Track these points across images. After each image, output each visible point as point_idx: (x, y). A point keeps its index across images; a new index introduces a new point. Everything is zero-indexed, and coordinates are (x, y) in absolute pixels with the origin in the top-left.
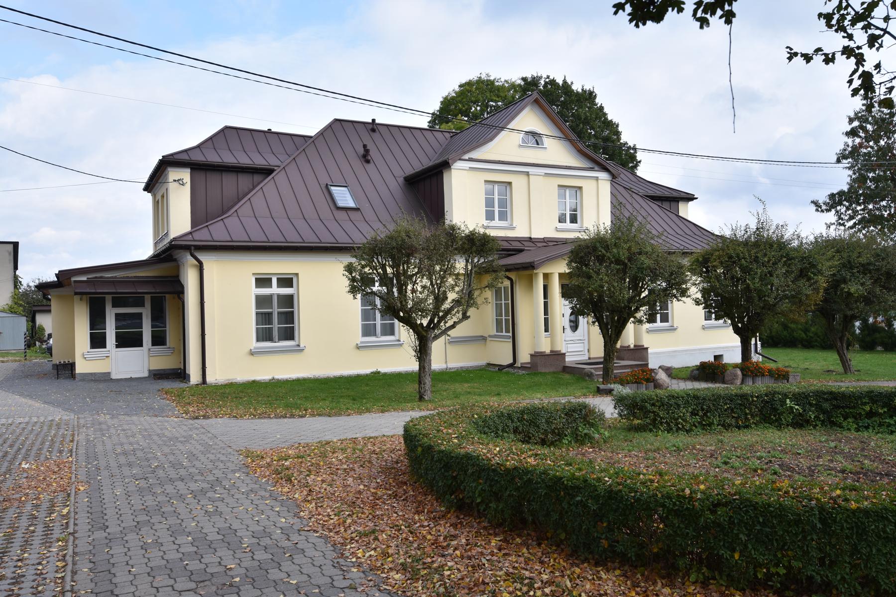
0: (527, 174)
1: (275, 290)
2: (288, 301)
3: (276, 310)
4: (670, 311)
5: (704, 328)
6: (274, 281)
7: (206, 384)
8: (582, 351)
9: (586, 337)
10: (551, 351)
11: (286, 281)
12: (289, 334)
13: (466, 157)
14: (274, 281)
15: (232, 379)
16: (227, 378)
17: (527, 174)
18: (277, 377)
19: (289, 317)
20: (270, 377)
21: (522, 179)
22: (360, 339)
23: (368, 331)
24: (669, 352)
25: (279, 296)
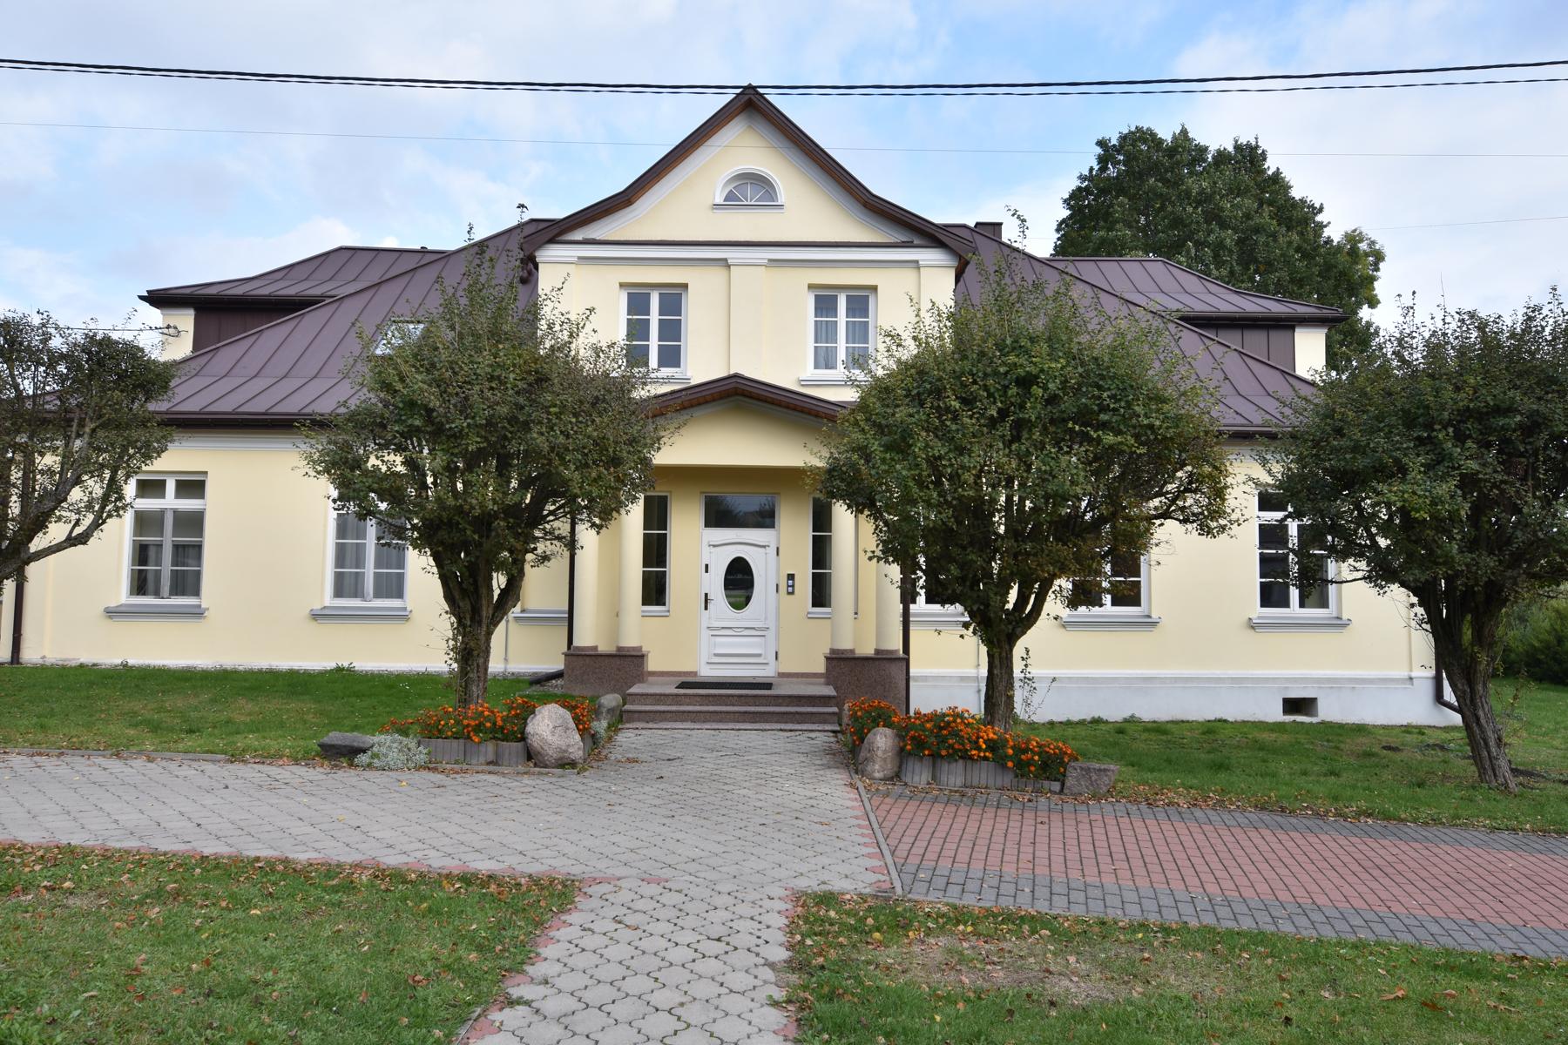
0: (725, 263)
1: (170, 501)
2: (192, 523)
3: (168, 539)
4: (1143, 579)
5: (1252, 626)
6: (171, 486)
7: (18, 663)
8: (759, 655)
9: (771, 624)
10: (878, 651)
11: (192, 486)
12: (187, 584)
13: (578, 235)
14: (171, 486)
15: (70, 660)
16: (64, 657)
17: (725, 263)
18: (131, 662)
19: (190, 552)
20: (118, 661)
21: (715, 275)
22: (327, 599)
23: (345, 585)
24: (1129, 680)
25: (175, 512)
